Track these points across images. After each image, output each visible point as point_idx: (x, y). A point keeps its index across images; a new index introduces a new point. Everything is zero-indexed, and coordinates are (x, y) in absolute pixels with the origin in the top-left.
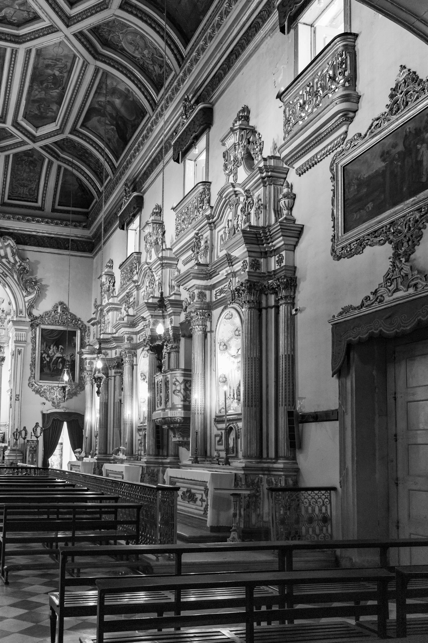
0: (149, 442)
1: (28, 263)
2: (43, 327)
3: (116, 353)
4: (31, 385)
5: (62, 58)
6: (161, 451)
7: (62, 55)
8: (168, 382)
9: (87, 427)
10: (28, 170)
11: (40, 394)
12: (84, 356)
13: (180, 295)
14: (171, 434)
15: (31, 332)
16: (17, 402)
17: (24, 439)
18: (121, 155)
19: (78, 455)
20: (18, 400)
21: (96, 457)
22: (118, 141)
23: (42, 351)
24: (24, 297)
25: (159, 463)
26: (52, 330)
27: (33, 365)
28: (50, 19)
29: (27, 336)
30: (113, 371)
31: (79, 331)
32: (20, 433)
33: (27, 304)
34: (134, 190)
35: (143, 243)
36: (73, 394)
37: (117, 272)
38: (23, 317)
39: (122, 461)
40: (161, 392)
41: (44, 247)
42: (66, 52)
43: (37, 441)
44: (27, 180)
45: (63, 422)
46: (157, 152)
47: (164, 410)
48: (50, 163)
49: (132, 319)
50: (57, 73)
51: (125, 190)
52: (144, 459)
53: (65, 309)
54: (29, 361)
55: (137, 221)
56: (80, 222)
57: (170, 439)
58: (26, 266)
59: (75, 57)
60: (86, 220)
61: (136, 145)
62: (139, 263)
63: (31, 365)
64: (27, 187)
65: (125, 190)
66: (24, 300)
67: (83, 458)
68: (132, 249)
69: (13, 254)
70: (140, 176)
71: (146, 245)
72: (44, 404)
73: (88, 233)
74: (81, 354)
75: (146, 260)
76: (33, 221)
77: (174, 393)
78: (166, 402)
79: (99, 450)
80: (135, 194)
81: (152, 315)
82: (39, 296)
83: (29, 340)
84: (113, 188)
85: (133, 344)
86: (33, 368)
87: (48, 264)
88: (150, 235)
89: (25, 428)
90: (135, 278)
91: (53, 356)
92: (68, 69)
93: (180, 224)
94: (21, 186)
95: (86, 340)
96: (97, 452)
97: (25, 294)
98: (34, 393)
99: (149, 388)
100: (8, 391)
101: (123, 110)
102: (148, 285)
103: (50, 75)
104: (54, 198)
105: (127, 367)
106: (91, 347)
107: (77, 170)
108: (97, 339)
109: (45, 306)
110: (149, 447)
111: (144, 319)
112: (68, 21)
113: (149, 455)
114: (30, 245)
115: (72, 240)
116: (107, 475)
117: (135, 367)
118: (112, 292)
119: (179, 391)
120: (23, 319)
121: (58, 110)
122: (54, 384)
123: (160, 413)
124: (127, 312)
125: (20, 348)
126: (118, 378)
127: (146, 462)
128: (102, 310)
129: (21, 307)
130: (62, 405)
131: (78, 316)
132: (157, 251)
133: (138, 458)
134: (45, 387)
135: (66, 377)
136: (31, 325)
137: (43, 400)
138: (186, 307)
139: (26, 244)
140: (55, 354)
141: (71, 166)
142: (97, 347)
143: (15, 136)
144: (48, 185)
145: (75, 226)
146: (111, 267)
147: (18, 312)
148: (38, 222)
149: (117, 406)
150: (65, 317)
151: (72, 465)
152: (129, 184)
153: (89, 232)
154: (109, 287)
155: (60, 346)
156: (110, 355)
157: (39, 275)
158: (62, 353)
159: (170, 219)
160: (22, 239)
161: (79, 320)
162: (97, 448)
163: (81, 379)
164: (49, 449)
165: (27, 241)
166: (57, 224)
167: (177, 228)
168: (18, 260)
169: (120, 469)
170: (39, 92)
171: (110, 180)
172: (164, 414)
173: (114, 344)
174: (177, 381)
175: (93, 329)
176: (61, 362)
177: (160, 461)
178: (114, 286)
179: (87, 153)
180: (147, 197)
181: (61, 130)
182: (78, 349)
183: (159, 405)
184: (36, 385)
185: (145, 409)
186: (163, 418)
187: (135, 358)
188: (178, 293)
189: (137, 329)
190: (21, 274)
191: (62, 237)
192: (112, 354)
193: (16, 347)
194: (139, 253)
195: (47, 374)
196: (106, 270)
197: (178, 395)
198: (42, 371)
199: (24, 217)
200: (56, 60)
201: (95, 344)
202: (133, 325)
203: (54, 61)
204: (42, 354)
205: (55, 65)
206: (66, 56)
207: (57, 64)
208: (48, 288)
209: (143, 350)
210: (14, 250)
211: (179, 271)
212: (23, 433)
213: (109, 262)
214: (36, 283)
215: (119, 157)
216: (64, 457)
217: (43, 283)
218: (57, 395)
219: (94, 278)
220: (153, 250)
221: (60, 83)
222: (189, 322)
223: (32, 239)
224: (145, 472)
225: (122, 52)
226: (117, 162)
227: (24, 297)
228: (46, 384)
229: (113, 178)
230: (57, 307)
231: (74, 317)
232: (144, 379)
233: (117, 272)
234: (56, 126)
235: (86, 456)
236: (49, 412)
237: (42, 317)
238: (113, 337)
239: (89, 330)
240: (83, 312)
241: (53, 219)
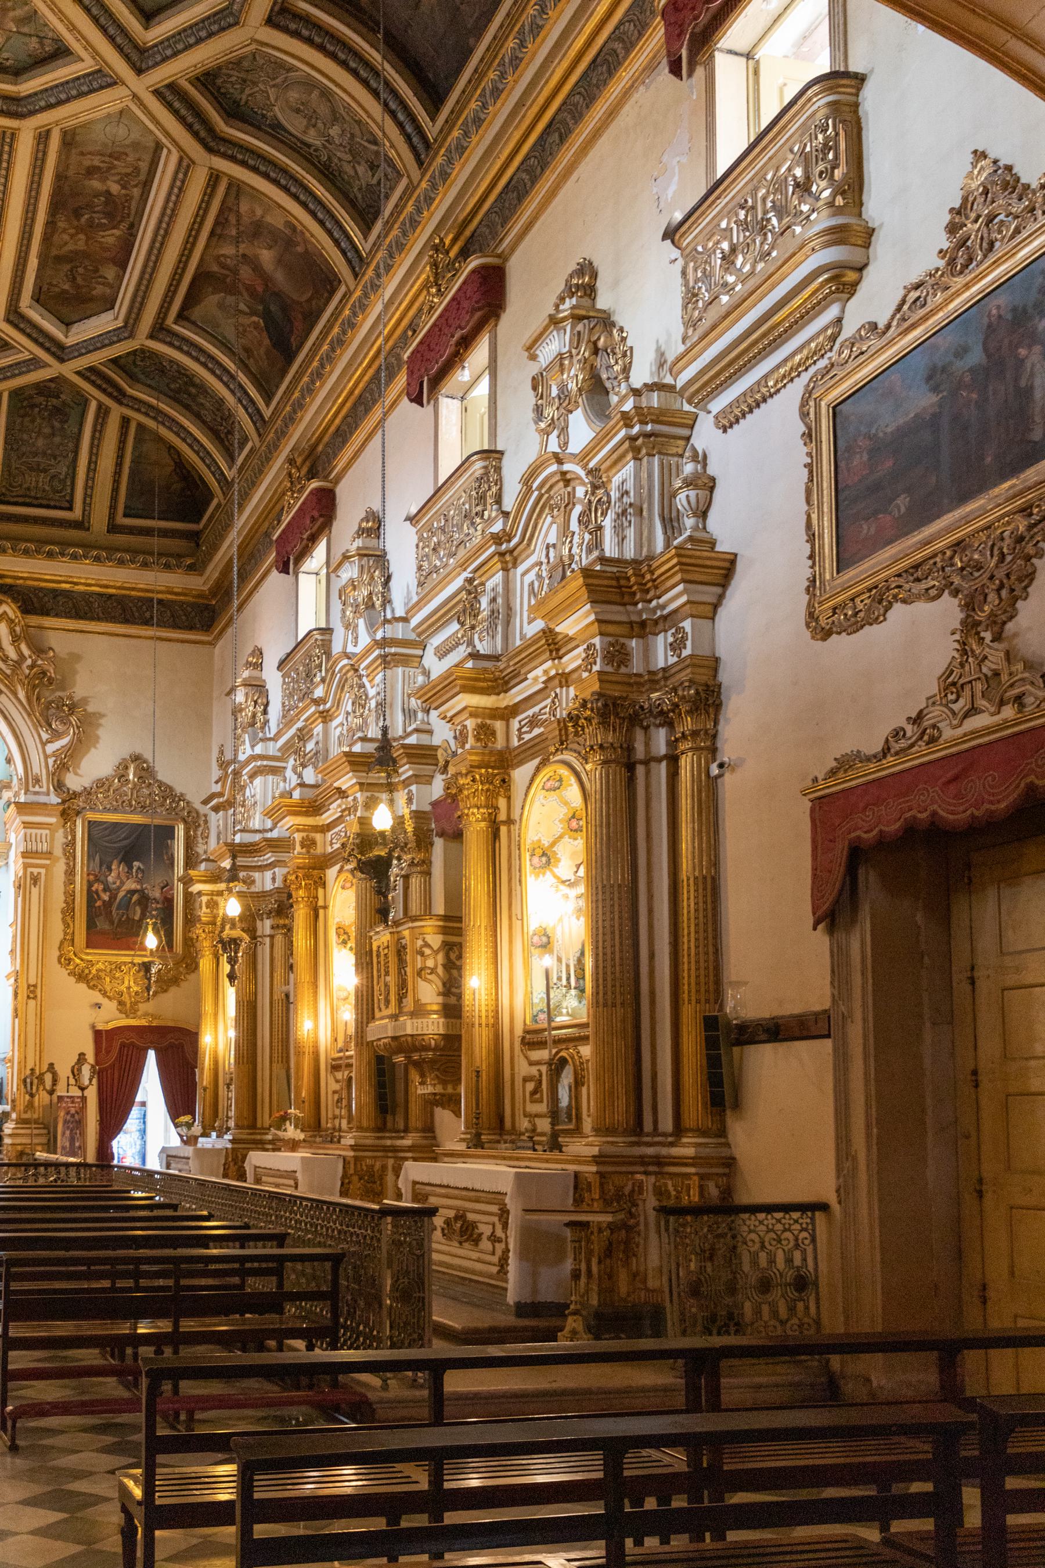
0: (358, 1097)
1: (53, 661)
2: (91, 816)
3: (274, 879)
4: (64, 960)
5: (127, 150)
6: (389, 1118)
7: (127, 142)
8: (404, 947)
9: (207, 1062)
10: (47, 430)
11: (88, 983)
12: (196, 888)
13: (430, 732)
14: (415, 1076)
15: (61, 831)
16: (32, 1002)
17: (51, 1092)
18: (278, 387)
19: (184, 1131)
20: (35, 998)
21: (228, 1137)
22: (267, 353)
23: (92, 877)
24: (44, 744)
25: (386, 1149)
26: (116, 825)
27: (69, 910)
28: (96, 54)
29: (52, 839)
30: (268, 923)
31: (182, 826)
32: (41, 1079)
33: (51, 761)
34: (312, 475)
35: (337, 606)
36: (168, 982)
37: (273, 680)
39: (293, 1145)
40: (387, 973)
41: (92, 619)
42: (135, 135)
43: (84, 1099)
44: (44, 454)
45: (146, 1050)
46: (366, 378)
47: (394, 1017)
48: (103, 413)
49: (311, 793)
50: (115, 188)
51: (290, 475)
52: (348, 1140)
53: (146, 772)
54: (58, 900)
55: (320, 551)
56: (179, 556)
57: (412, 1090)
58: (46, 667)
59: (158, 147)
60: (193, 551)
61: (315, 364)
62: (328, 654)
63: (63, 912)
64: (45, 471)
65: (290, 475)
67: (196, 1138)
68: (308, 620)
69: (16, 640)
70: (326, 439)
71: (344, 611)
72: (99, 1006)
73: (198, 583)
74: (187, 881)
75: (345, 646)
76: (63, 555)
77: (419, 974)
78: (400, 999)
79: (238, 1118)
80: (314, 484)
81: (361, 784)
82: (80, 741)
83: (58, 851)
84: (260, 472)
85: (315, 857)
86: (68, 919)
87: (101, 662)
88: (353, 584)
89: (51, 1065)
90: (319, 692)
91: (119, 888)
92: (142, 177)
93: (427, 556)
94: (31, 469)
95: (200, 849)
96: (232, 1123)
97: (45, 736)
98: (73, 979)
99: (357, 965)
100: (8, 977)
101: (280, 277)
102: (349, 708)
103: (97, 195)
104: (114, 498)
105: (301, 914)
106: (211, 865)
107: (170, 429)
108: (226, 844)
109: (97, 765)
110: (359, 1108)
111: (342, 793)
112: (140, 58)
113: (360, 1128)
114: (57, 615)
115: (160, 602)
116: (258, 1181)
117: (321, 912)
118: (262, 728)
119: (433, 971)
120: (42, 799)
121: (120, 278)
122: (123, 957)
123: (385, 1027)
124: (300, 776)
126: (279, 939)
127: (353, 1148)
128: (237, 774)
129: (36, 770)
130: (143, 1007)
131: (178, 789)
132: (371, 627)
133: (333, 1138)
134: (100, 966)
135: (151, 941)
137: (96, 997)
138: (447, 762)
139: (48, 615)
140: (123, 883)
141: (154, 418)
142: (227, 864)
143: (14, 347)
144: (98, 468)
145: (167, 567)
146: (258, 666)
147: (30, 781)
148: (74, 557)
149: (278, 1009)
150: (146, 791)
151: (169, 1157)
152: (299, 461)
153: (200, 580)
154: (254, 715)
155: (136, 864)
156: (258, 883)
157: (79, 690)
158: (139, 881)
159: (402, 545)
160: (35, 601)
161: (181, 797)
162: (232, 1114)
163: (189, 943)
164: (113, 1118)
165: (49, 605)
166: (121, 562)
167: (420, 568)
168: (26, 652)
169: (290, 1165)
170: (72, 236)
171: (252, 451)
172: (395, 1028)
173: (269, 857)
174: (427, 945)
175: (216, 820)
176: (139, 902)
177: (389, 1142)
178: (265, 712)
179: (194, 385)
180: (342, 491)
181: (128, 329)
182: (179, 869)
183: (382, 1006)
184: (78, 961)
185: (348, 1015)
186: (395, 1038)
187: (321, 891)
188: (426, 727)
189: (327, 818)
190: (34, 687)
191: (133, 593)
192: (266, 882)
194: (327, 631)
195: (103, 933)
196: (246, 674)
197: (429, 981)
198: (91, 924)
199: (40, 548)
200: (110, 156)
201: (221, 857)
202: (314, 808)
203: (107, 159)
204: (90, 884)
205: (109, 169)
206: (136, 145)
207: (114, 167)
208: (102, 721)
209: (340, 871)
210: (18, 629)
211: (426, 673)
212: (48, 1078)
213: (253, 654)
214: (72, 708)
215: (274, 394)
216: (149, 1137)
217: (90, 709)
218: (130, 983)
219: (215, 695)
220: (361, 622)
221: (123, 214)
222: (454, 798)
223: (61, 600)
224: (352, 1171)
225: (275, 132)
226: (268, 405)
227: (44, 744)
228: (101, 959)
229: (258, 445)
230: (127, 768)
231: (168, 792)
232: (344, 942)
233: (273, 680)
234: (116, 319)
235: (205, 1135)
236: (111, 1026)
237: (89, 793)
238: (266, 840)
239: (206, 822)
240: (191, 779)
241: (111, 549)
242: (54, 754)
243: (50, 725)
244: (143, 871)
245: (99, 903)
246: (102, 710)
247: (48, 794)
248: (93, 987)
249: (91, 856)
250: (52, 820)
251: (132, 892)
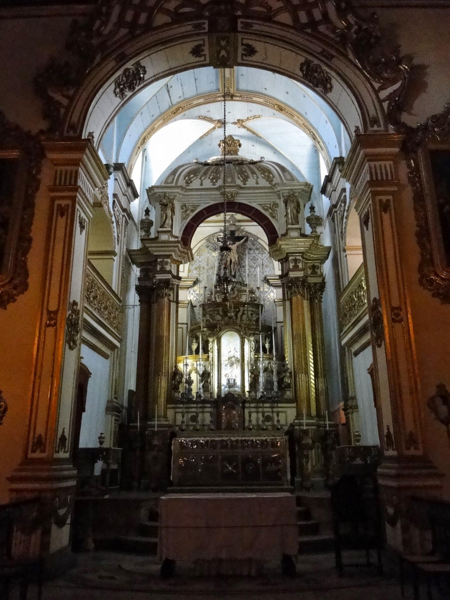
27: (423, 234)
29: (396, 169)
33: (385, 105)
66: (378, 97)
97: (377, 85)
98: (437, 301)
125: (384, 198)
129: (372, 112)
193: (374, 194)
227: (376, 92)
242: (389, 97)
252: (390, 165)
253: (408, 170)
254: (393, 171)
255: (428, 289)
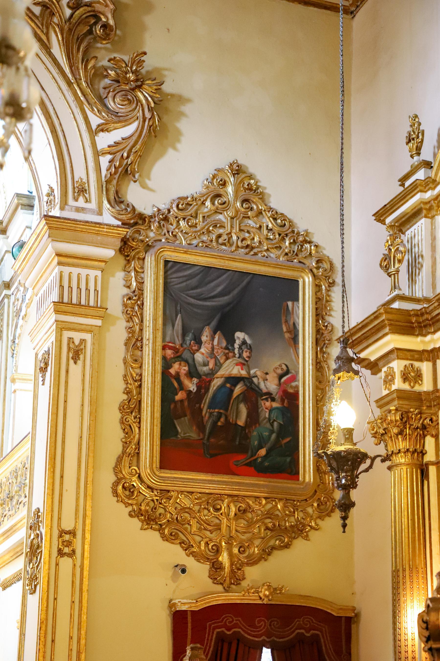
4: (124, 490)
11: (161, 529)
15: (120, 275)
23: (169, 353)
27: (131, 407)
31: (308, 279)
33: (105, 161)
38: (91, 211)
53: (251, 193)
54: (114, 392)
63: (122, 408)
66: (94, 144)
83: (115, 306)
86: (131, 419)
91: (212, 373)
97: (95, 121)
98: (136, 523)
125: (77, 336)
129: (80, 173)
130: (253, 574)
131: (301, 226)
136: (125, 248)
137: (175, 553)
140: (218, 365)
155: (240, 336)
190: (80, 40)
193: (61, 327)
195: (187, 443)
204: (167, 364)
208: (186, 108)
230: (224, 184)
231: (285, 228)
237: (166, 219)
243: (105, 106)
244: (250, 348)
245: (180, 396)
246: (186, 93)
247: (100, 213)
248: (170, 538)
249: (168, 319)
250: (109, 253)
251: (234, 380)
252: (96, 277)
253: (126, 291)
254: (99, 288)
255: (125, 503)
